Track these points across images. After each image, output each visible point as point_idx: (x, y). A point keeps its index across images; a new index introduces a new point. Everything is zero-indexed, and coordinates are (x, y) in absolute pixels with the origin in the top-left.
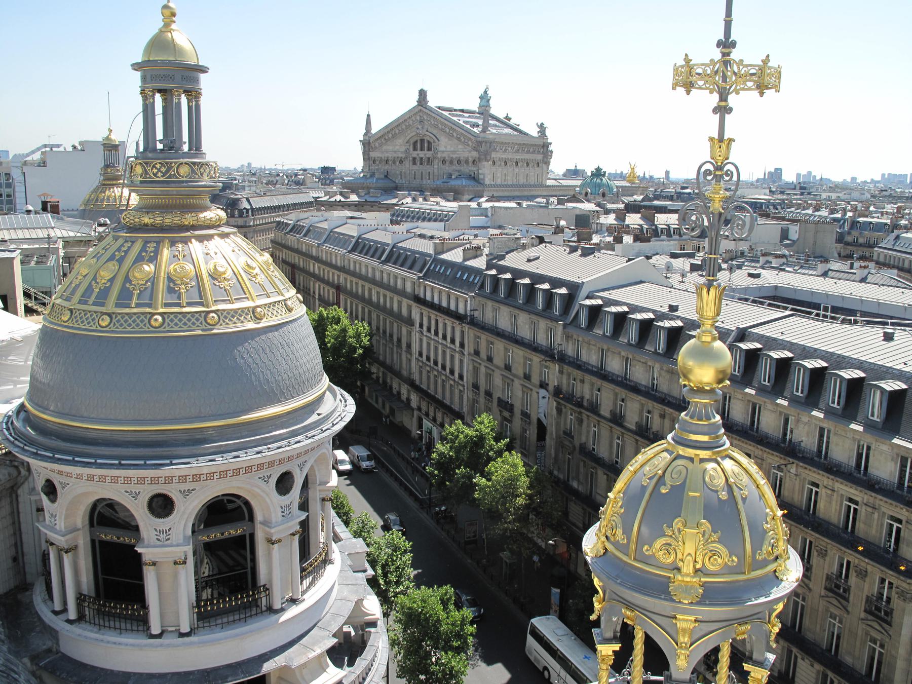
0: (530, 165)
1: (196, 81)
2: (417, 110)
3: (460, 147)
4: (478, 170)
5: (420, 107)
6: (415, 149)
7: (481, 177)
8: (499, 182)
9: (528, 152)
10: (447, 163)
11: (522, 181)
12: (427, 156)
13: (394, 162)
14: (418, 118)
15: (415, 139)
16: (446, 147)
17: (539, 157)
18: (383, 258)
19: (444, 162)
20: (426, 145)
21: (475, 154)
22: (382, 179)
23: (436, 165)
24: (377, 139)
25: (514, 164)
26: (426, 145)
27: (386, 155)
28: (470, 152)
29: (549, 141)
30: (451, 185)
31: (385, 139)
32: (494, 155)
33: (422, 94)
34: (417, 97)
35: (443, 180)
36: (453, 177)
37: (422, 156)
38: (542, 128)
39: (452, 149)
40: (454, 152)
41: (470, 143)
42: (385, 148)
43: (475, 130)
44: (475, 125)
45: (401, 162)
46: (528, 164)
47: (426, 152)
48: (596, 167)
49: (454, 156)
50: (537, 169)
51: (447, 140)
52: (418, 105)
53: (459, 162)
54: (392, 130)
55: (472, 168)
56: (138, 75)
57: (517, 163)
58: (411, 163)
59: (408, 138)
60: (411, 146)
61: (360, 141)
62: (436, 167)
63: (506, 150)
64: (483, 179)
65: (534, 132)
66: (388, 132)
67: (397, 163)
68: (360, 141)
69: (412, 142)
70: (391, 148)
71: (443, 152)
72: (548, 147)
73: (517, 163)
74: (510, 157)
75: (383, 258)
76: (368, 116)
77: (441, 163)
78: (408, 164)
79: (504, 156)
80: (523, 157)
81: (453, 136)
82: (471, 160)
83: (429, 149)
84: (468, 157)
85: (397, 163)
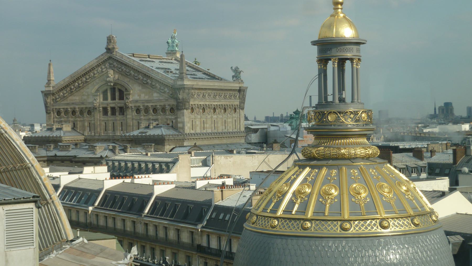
0: (227, 111)
1: (358, 50)
2: (106, 58)
3: (155, 95)
4: (176, 118)
5: (109, 55)
6: (105, 98)
7: (180, 125)
8: (198, 131)
9: (225, 97)
10: (142, 112)
11: (221, 128)
12: (119, 105)
13: (82, 112)
14: (107, 65)
15: (105, 88)
16: (139, 96)
17: (237, 102)
18: (147, 211)
19: (138, 111)
20: (117, 94)
21: (173, 102)
22: (69, 132)
23: (131, 114)
24: (61, 90)
25: (212, 111)
26: (117, 94)
27: (72, 107)
28: (167, 100)
29: (244, 85)
30: (150, 136)
31: (71, 89)
32: (191, 103)
33: (110, 40)
34: (104, 44)
35: (140, 130)
36: (151, 127)
37: (113, 105)
38: (237, 74)
39: (147, 98)
40: (148, 101)
41: (166, 89)
42: (70, 98)
43: (170, 75)
44: (167, 71)
45: (89, 112)
46: (225, 110)
47: (117, 100)
48: (295, 110)
49: (150, 105)
50: (234, 115)
51: (140, 88)
52: (107, 52)
53: (155, 110)
54: (78, 79)
55: (170, 117)
56: (316, 48)
57: (215, 109)
58: (101, 113)
59: (97, 87)
60: (102, 96)
61: (42, 92)
62: (128, 116)
63: (204, 96)
64: (183, 128)
65: (228, 75)
66: (74, 81)
67: (86, 114)
68: (42, 92)
69: (101, 90)
70: (77, 98)
71: (137, 101)
72: (244, 91)
73: (215, 109)
74: (207, 103)
75: (147, 211)
76: (50, 65)
77: (135, 113)
78: (98, 116)
79: (202, 103)
80: (220, 103)
81: (147, 83)
82: (168, 108)
83: (121, 98)
84: (165, 105)
85: (86, 114)
